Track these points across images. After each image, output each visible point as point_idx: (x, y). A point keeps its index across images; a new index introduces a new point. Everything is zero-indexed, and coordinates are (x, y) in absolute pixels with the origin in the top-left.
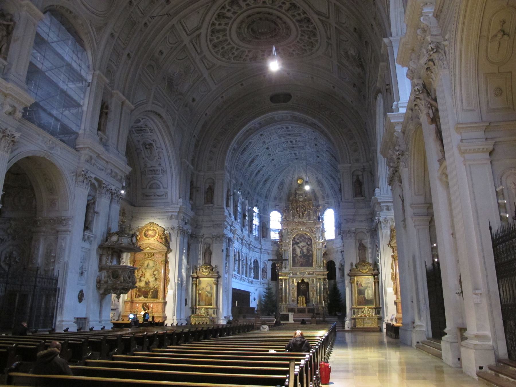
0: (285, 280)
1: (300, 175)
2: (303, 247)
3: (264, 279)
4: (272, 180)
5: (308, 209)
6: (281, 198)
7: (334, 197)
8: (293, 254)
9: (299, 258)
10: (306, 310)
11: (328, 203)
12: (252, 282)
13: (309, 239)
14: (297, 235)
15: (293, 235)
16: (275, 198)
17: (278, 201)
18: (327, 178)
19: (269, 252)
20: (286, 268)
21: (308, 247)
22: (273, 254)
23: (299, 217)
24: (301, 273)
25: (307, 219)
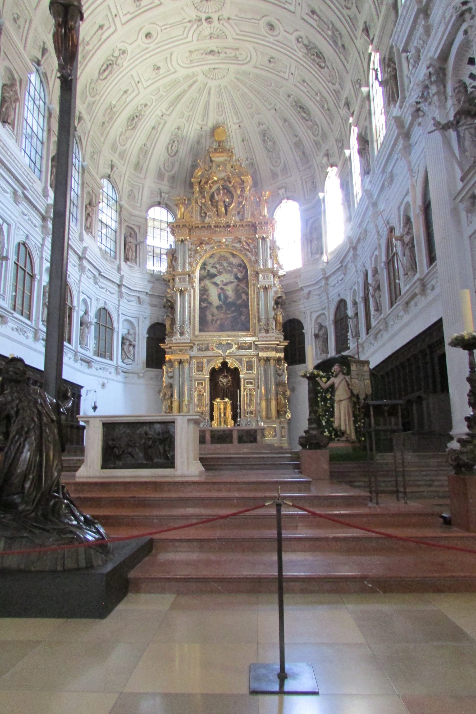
0: (180, 362)
1: (221, 119)
2: (226, 284)
3: (127, 361)
4: (152, 123)
5: (239, 197)
6: (173, 177)
7: (302, 168)
8: (201, 300)
9: (215, 311)
10: (235, 436)
11: (285, 188)
12: (88, 362)
13: (240, 265)
14: (211, 257)
15: (201, 257)
16: (160, 176)
17: (165, 182)
18: (285, 120)
19: (142, 296)
20: (182, 334)
21: (238, 285)
22: (152, 305)
23: (218, 215)
24: (220, 345)
25: (237, 219)
